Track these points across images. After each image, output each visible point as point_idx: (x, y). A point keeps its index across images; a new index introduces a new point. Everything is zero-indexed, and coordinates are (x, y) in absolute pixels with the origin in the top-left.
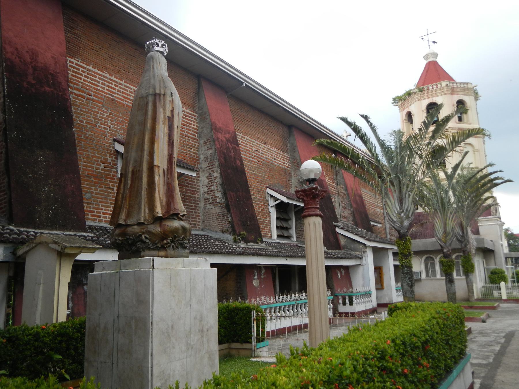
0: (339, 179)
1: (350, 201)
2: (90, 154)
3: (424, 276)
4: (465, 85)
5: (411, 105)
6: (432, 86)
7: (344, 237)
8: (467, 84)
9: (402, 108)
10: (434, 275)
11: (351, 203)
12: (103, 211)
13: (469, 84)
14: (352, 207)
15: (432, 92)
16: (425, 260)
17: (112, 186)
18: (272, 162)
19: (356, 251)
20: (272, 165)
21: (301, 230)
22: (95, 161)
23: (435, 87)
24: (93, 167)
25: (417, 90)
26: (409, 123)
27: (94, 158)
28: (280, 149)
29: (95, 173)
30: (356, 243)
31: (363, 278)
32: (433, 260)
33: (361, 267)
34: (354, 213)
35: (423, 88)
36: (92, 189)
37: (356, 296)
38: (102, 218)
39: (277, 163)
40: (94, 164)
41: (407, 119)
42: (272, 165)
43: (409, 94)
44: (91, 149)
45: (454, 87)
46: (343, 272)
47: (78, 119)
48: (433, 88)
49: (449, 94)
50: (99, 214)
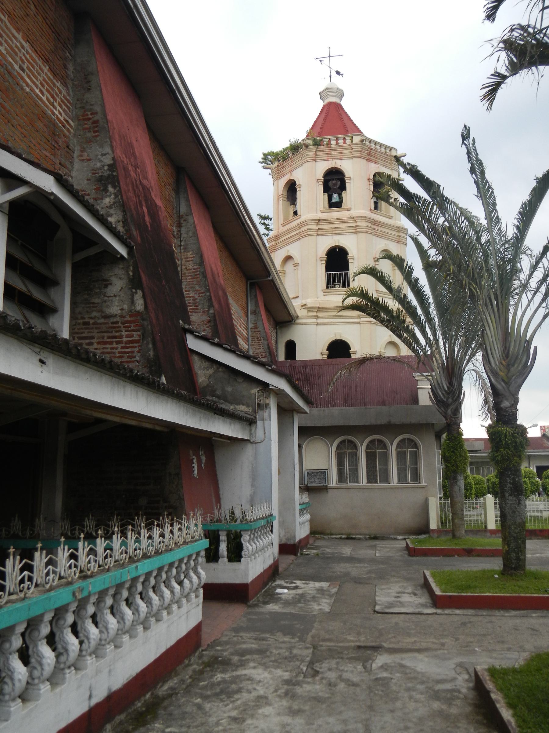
0: (184, 235)
1: (209, 290)
3: (333, 481)
4: (388, 151)
5: (296, 168)
6: (337, 139)
7: (206, 364)
8: (391, 149)
9: (277, 175)
10: (355, 479)
11: (210, 296)
13: (393, 150)
14: (211, 305)
15: (335, 150)
16: (338, 447)
18: (10, 67)
19: (238, 404)
20: (10, 80)
21: (85, 324)
23: (341, 141)
25: (310, 142)
26: (289, 203)
28: (46, 61)
30: (240, 380)
31: (254, 477)
32: (355, 447)
33: (249, 451)
34: (215, 320)
35: (321, 140)
37: (252, 530)
39: (28, 85)
41: (285, 194)
42: (10, 80)
43: (295, 148)
45: (371, 149)
46: (203, 458)
48: (337, 143)
49: (364, 158)
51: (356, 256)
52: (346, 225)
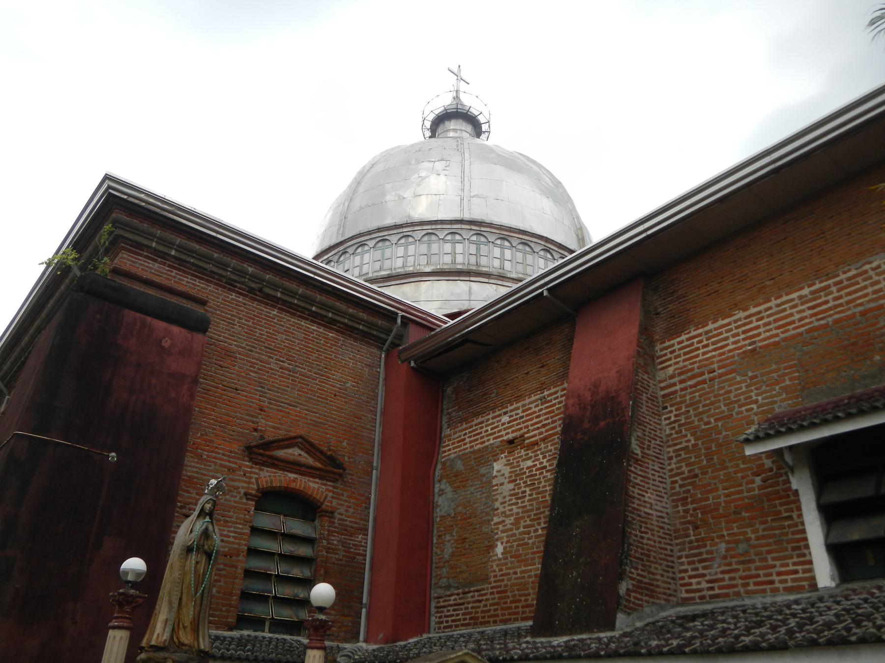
2: (730, 470)
12: (778, 569)
17: (786, 512)
22: (743, 477)
24: (741, 492)
27: (740, 475)
29: (746, 501)
36: (746, 533)
38: (777, 585)
40: (741, 485)
44: (730, 461)
47: (702, 423)
50: (770, 578)
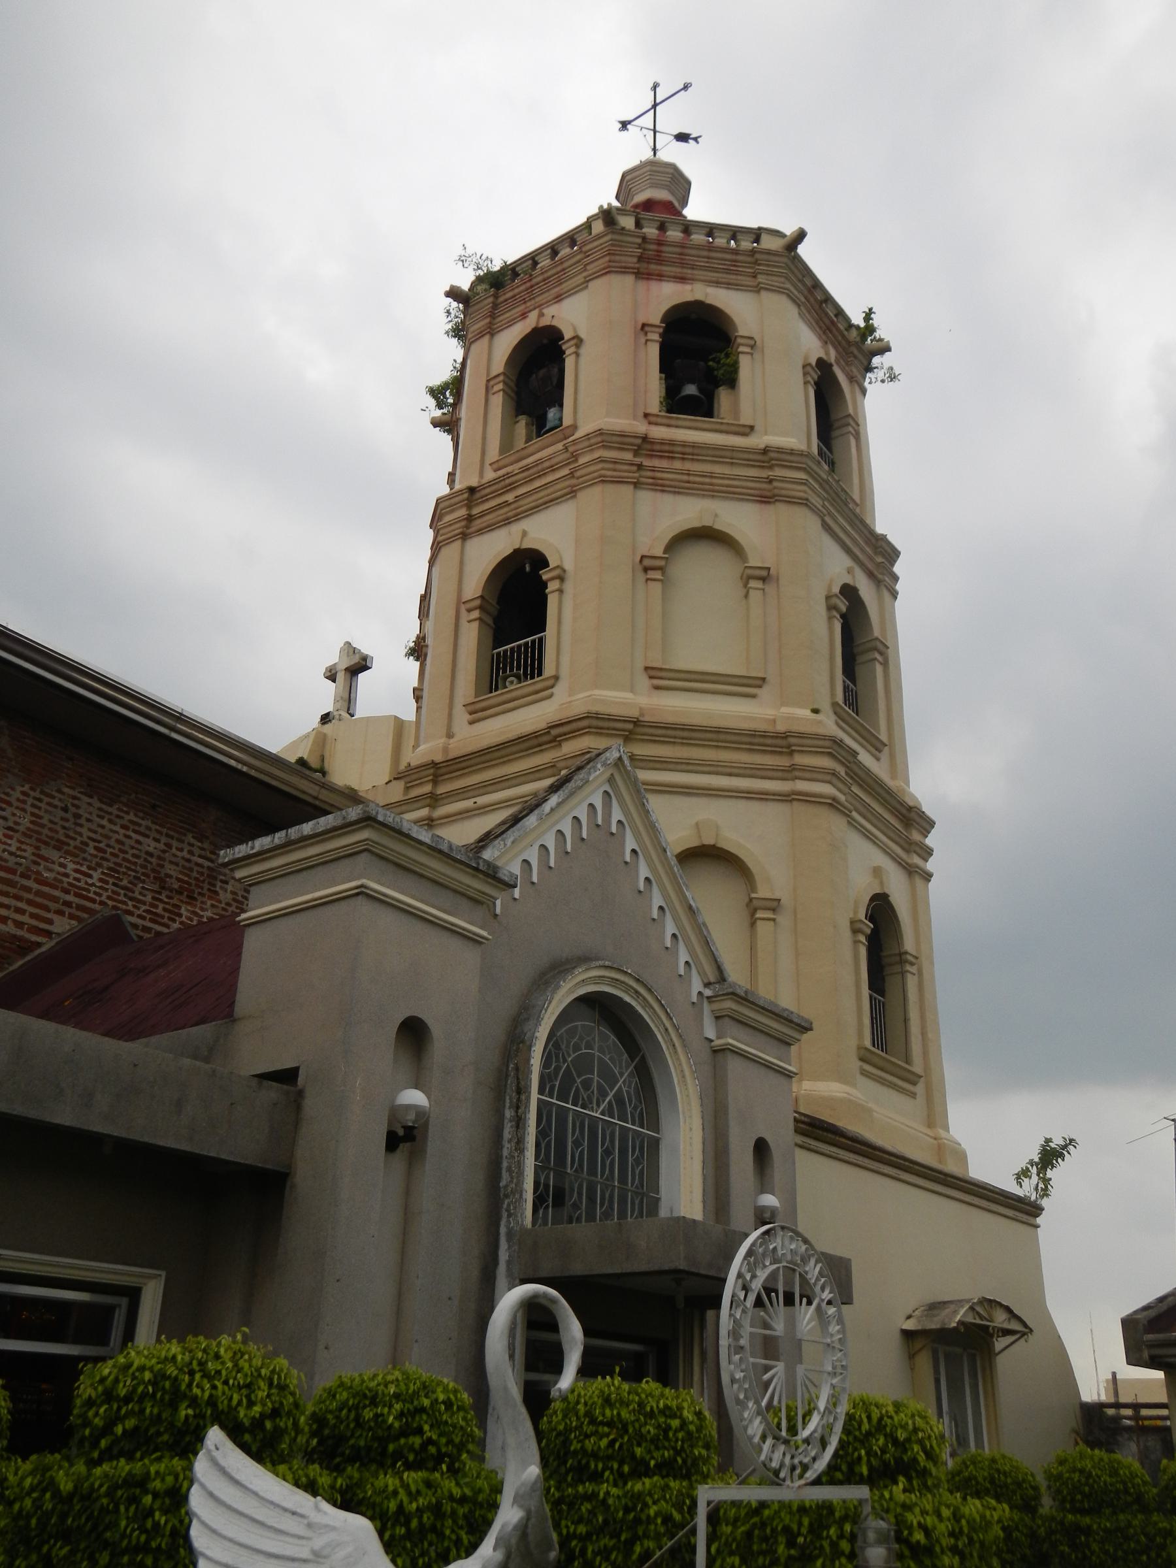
8: (757, 234)
49: (624, 270)
51: (568, 565)
52: (549, 478)
